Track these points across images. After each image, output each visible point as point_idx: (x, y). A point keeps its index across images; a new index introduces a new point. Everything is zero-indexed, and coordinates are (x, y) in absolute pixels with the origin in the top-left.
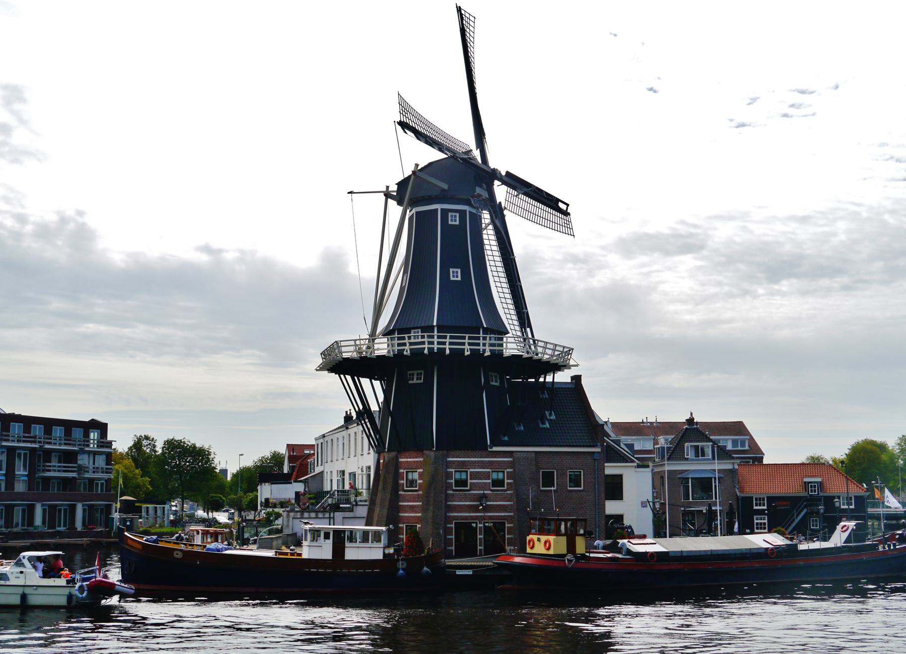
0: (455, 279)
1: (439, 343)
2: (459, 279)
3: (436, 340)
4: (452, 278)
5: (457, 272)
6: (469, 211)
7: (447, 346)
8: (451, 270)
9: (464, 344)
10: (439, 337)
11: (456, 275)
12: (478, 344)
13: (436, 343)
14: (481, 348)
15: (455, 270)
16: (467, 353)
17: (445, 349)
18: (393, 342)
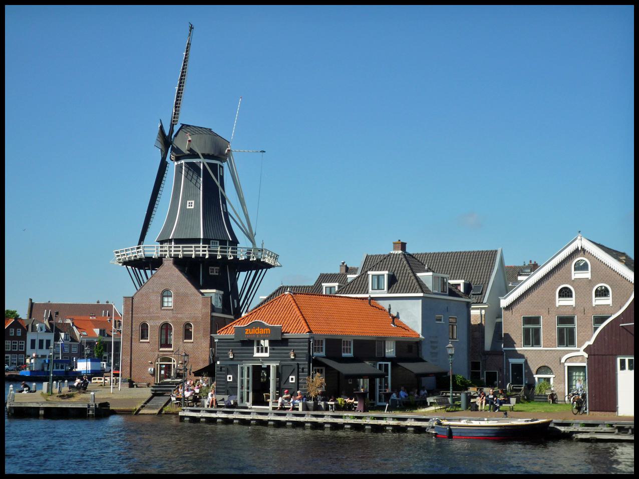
1: (175, 251)
2: (193, 207)
3: (173, 249)
5: (192, 203)
8: (188, 202)
9: (192, 251)
10: (175, 247)
11: (191, 205)
13: (173, 251)
14: (201, 253)
15: (191, 202)
18: (171, 249)
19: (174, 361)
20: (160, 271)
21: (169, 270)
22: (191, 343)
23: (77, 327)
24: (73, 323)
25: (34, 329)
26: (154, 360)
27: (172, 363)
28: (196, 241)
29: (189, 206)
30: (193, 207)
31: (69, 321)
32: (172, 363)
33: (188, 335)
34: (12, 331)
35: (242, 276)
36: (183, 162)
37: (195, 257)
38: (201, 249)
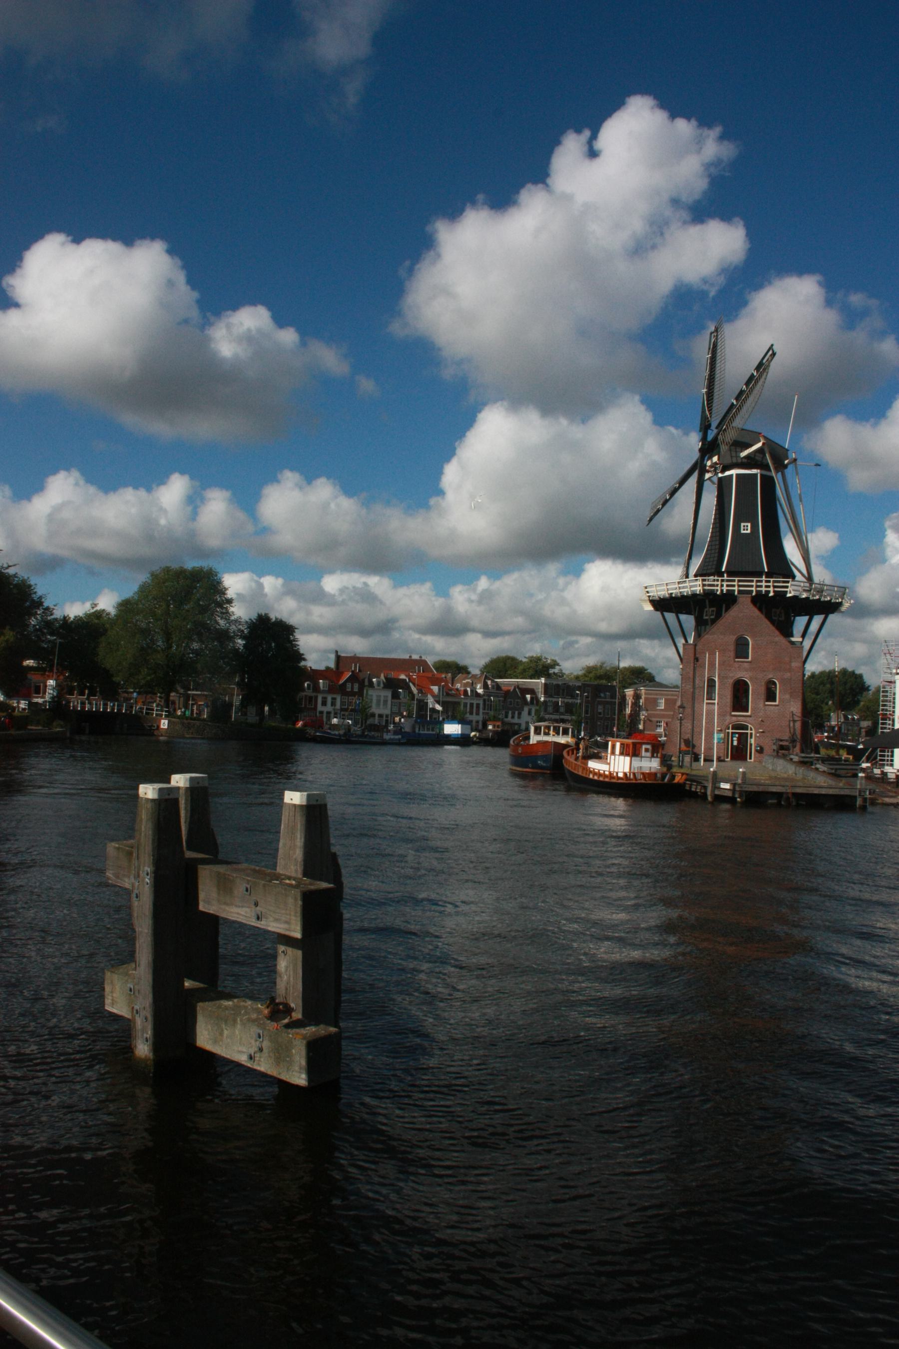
0: (745, 532)
1: (727, 586)
2: (749, 531)
4: (743, 532)
6: (761, 475)
7: (736, 588)
8: (742, 524)
9: (752, 586)
12: (761, 586)
14: (764, 589)
15: (746, 524)
16: (771, 594)
17: (734, 590)
19: (751, 730)
20: (734, 612)
21: (745, 610)
22: (776, 706)
23: (414, 684)
24: (409, 679)
25: (371, 684)
26: (723, 727)
27: (749, 731)
28: (759, 574)
29: (744, 530)
30: (749, 531)
31: (403, 677)
32: (749, 731)
33: (770, 695)
34: (349, 685)
35: (800, 622)
36: (733, 472)
37: (756, 595)
38: (764, 584)
